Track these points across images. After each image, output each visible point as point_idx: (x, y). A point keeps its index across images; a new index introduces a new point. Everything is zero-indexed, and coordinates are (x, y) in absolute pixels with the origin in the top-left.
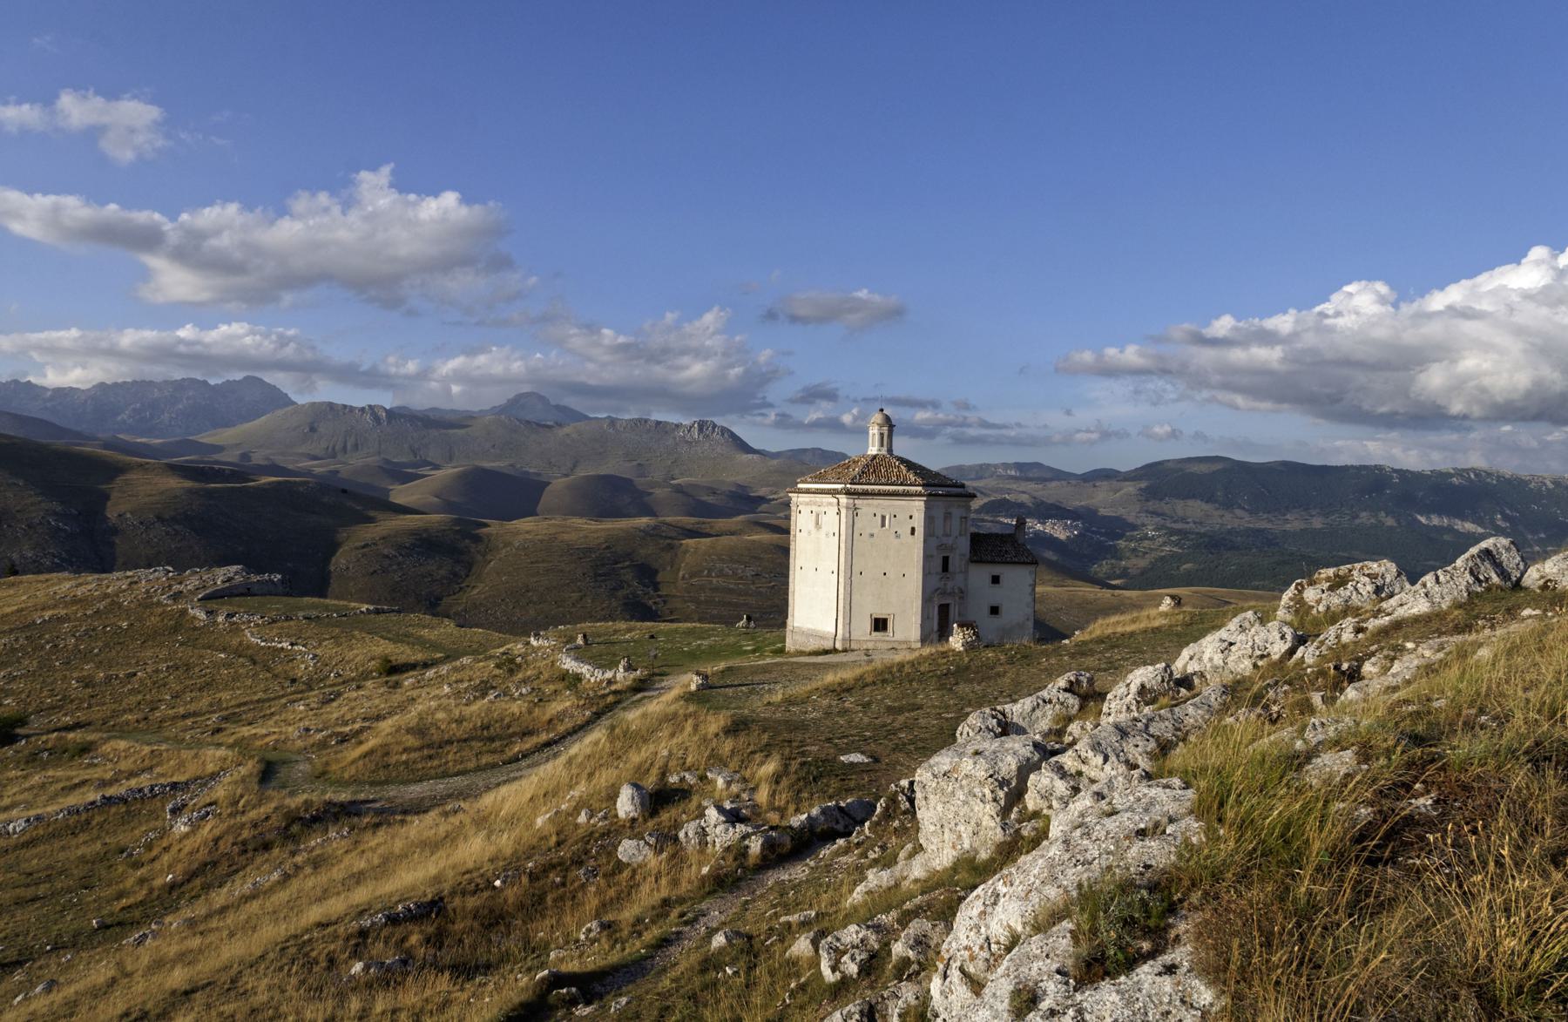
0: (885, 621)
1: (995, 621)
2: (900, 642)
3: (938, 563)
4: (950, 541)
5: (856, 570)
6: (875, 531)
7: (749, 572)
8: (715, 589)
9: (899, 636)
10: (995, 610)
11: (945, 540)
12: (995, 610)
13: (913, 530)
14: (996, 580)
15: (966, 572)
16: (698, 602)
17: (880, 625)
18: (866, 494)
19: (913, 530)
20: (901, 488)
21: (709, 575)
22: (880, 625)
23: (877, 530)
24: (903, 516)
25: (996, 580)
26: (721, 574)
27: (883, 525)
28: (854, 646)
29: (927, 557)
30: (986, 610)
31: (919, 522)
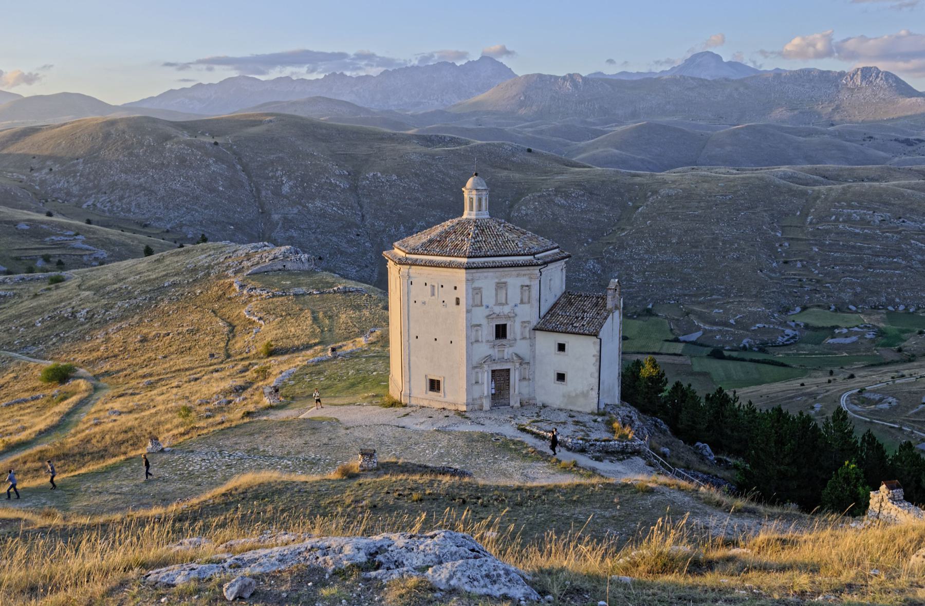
0: (439, 382)
1: (561, 387)
2: (450, 404)
3: (488, 332)
4: (506, 310)
5: (413, 333)
6: (427, 300)
7: (877, 218)
8: (841, 233)
9: (450, 398)
10: (561, 377)
11: (497, 310)
12: (561, 377)
13: (458, 299)
14: (562, 347)
15: (532, 339)
16: (821, 245)
17: (434, 385)
18: (414, 263)
19: (458, 299)
20: (449, 259)
21: (837, 220)
22: (434, 385)
23: (427, 298)
24: (448, 287)
25: (562, 347)
26: (849, 220)
27: (433, 294)
28: (413, 402)
29: (473, 327)
30: (553, 377)
31: (462, 293)
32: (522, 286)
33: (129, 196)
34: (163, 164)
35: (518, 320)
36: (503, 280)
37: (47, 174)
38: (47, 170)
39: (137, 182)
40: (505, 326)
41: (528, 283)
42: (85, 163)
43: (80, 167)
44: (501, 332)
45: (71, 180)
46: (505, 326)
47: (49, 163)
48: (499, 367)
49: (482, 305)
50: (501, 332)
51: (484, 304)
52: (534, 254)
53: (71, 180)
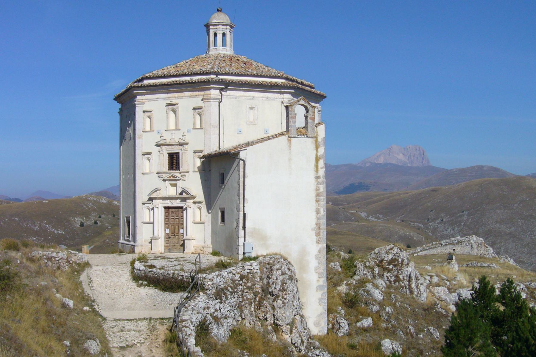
32: (194, 109)
33: (501, 242)
34: (532, 215)
35: (190, 149)
36: (175, 101)
37: (439, 223)
38: (439, 220)
39: (508, 231)
40: (177, 154)
41: (201, 104)
42: (469, 215)
43: (465, 218)
44: (174, 161)
45: (456, 228)
46: (177, 154)
47: (442, 215)
48: (170, 205)
49: (152, 131)
50: (174, 161)
51: (155, 129)
52: (217, 74)
53: (456, 228)
